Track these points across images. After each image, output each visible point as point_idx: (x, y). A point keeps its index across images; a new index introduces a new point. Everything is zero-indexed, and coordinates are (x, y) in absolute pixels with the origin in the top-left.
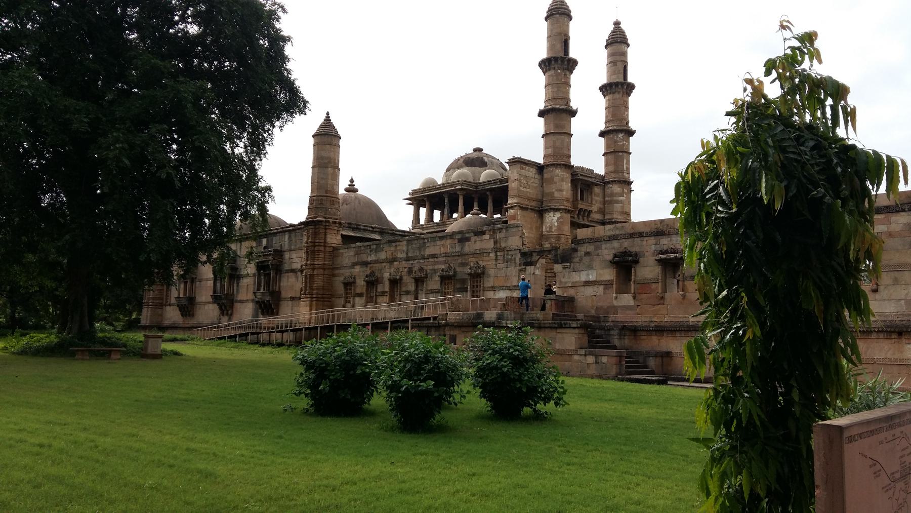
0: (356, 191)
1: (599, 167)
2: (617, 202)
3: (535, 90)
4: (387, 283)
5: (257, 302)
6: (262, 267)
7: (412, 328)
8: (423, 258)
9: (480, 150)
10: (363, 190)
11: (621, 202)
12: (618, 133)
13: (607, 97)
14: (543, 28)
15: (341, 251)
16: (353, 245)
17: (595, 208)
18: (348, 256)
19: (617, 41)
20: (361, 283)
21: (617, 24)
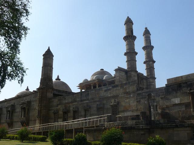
0: (60, 80)
1: (145, 74)
2: (152, 85)
3: (123, 47)
4: (72, 112)
5: (21, 122)
6: (23, 109)
7: (85, 132)
8: (88, 99)
9: (103, 70)
10: (62, 79)
11: (153, 85)
12: (150, 62)
13: (145, 51)
14: (124, 27)
15: (53, 100)
16: (57, 97)
17: (145, 87)
18: (56, 101)
19: (147, 33)
20: (61, 113)
21: (146, 28)
